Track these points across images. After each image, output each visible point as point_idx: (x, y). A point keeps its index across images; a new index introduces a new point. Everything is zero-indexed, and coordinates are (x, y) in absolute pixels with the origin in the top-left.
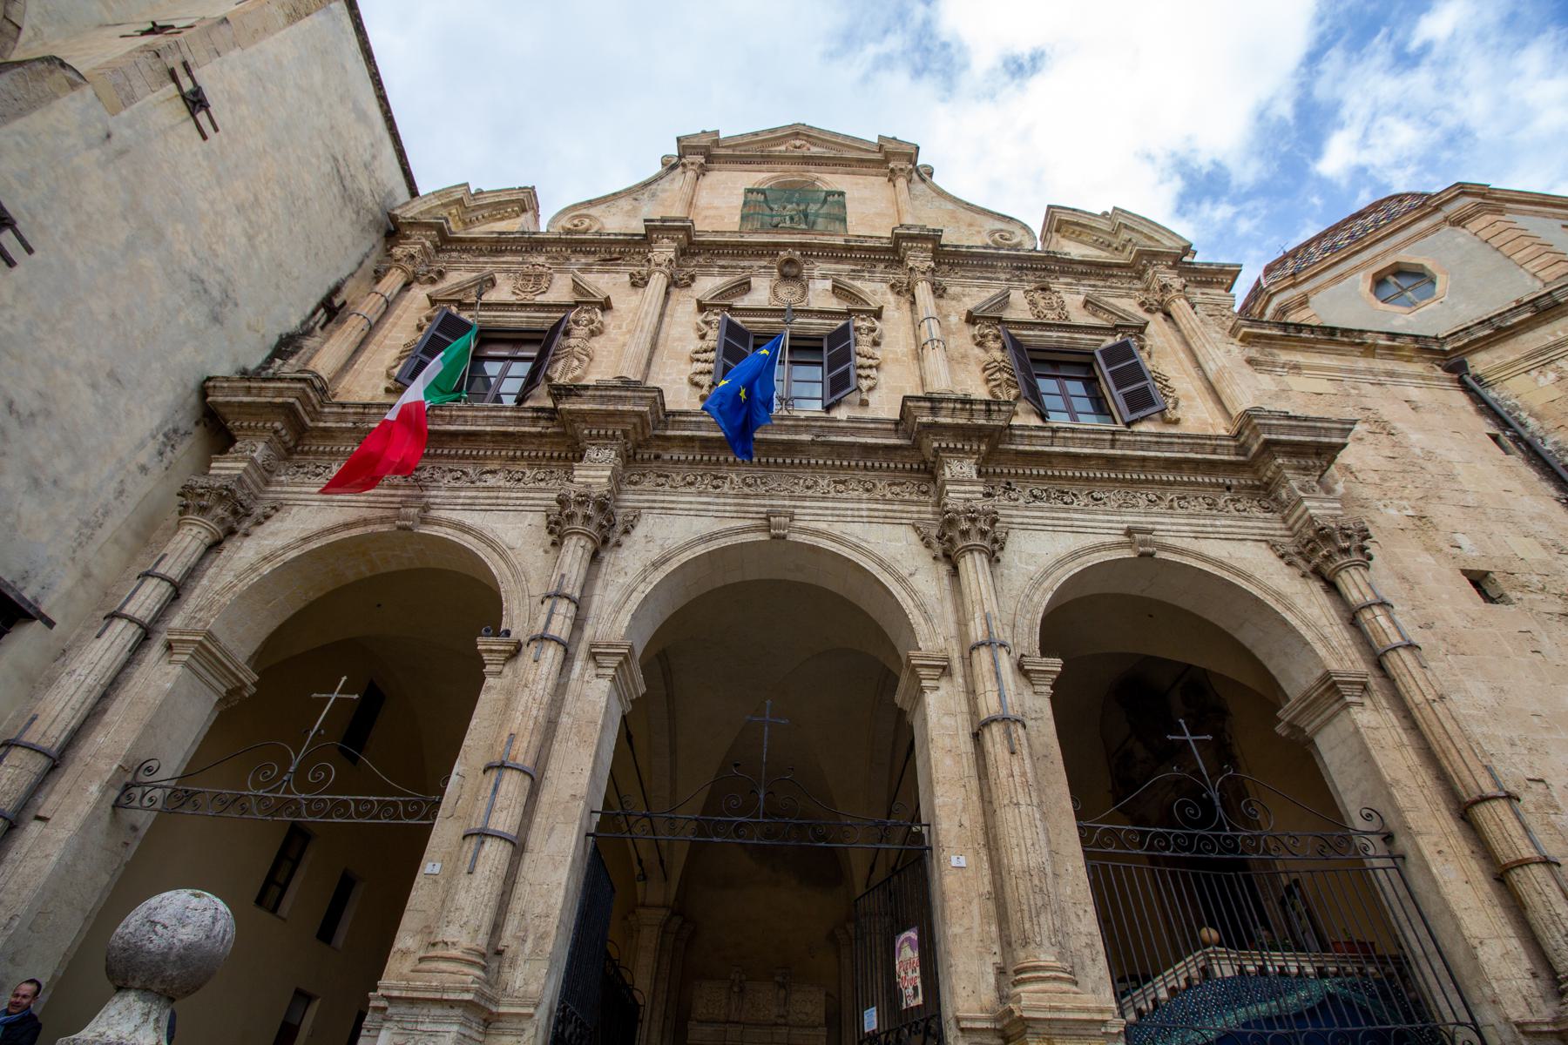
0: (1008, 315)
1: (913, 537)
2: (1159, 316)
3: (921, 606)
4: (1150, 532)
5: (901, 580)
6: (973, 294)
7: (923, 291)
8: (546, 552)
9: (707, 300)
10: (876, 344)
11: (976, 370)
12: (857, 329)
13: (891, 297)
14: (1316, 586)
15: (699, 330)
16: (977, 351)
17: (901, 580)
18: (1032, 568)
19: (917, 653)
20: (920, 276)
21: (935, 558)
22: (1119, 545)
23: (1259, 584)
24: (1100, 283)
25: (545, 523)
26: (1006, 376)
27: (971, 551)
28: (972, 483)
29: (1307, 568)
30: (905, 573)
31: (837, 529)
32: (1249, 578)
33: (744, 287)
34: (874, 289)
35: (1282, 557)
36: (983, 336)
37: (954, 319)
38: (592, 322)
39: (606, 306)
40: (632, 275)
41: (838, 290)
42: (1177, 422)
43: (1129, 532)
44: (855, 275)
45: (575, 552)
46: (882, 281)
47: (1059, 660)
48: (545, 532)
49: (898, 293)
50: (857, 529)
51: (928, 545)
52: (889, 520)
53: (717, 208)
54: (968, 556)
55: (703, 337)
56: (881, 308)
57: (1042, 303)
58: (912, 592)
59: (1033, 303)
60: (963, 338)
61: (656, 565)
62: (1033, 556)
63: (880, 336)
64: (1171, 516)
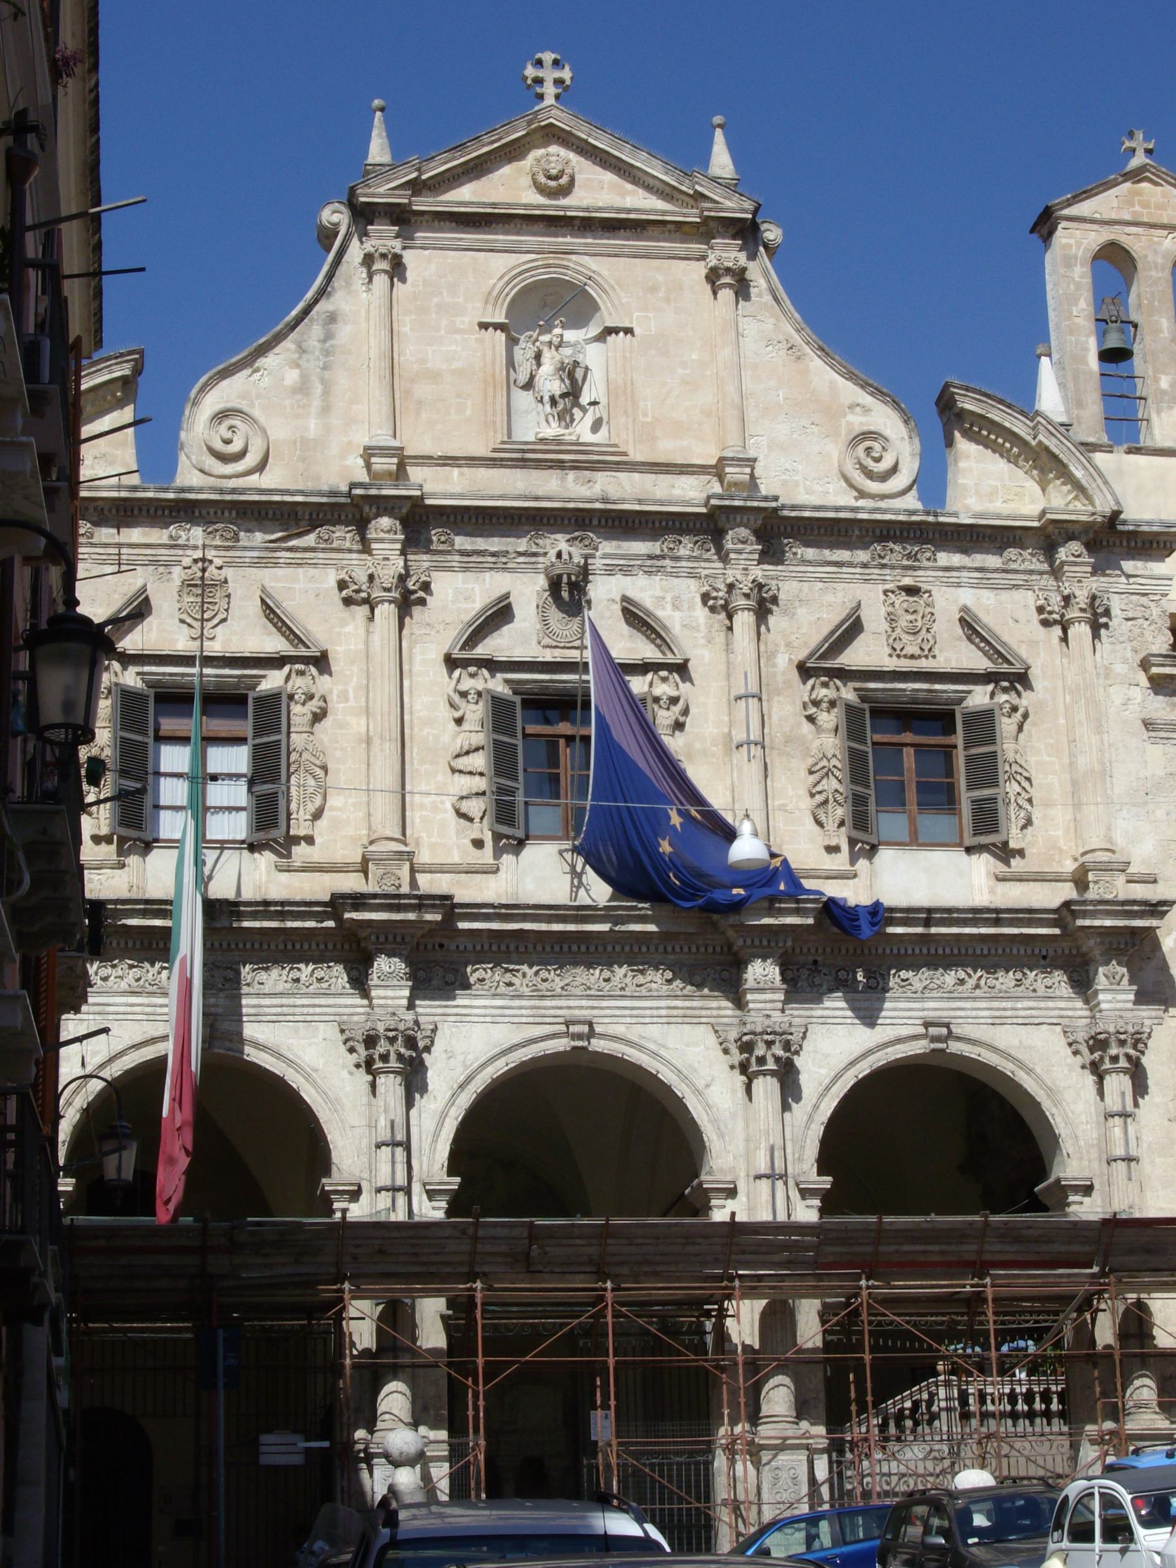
0: (856, 656)
1: (712, 1040)
2: (1057, 631)
3: (714, 1121)
4: (947, 1026)
5: (698, 1092)
6: (815, 596)
7: (744, 620)
8: (351, 1074)
9: (457, 654)
10: (679, 726)
11: (800, 766)
12: (657, 700)
13: (701, 614)
14: (1090, 1079)
15: (452, 705)
16: (807, 727)
17: (698, 1092)
18: (823, 1071)
19: (709, 1178)
20: (743, 602)
21: (732, 1067)
22: (915, 1037)
23: (1038, 1079)
24: (992, 561)
25: (340, 1038)
26: (835, 784)
27: (765, 1075)
28: (773, 990)
29: (1088, 1057)
30: (700, 1084)
31: (633, 1034)
32: (1030, 1071)
33: (500, 614)
34: (675, 594)
35: (1070, 1045)
36: (816, 703)
37: (783, 664)
38: (311, 697)
39: (321, 662)
40: (342, 585)
41: (636, 618)
42: (1021, 853)
43: (927, 1025)
44: (652, 565)
45: (391, 1087)
46: (693, 576)
47: (830, 1179)
48: (343, 1049)
49: (713, 609)
50: (654, 1031)
51: (726, 1051)
52: (689, 1019)
53: (434, 377)
54: (761, 1078)
55: (459, 721)
56: (687, 661)
57: (904, 621)
58: (708, 1106)
59: (891, 619)
60: (788, 701)
61: (462, 1086)
62: (827, 1056)
63: (686, 712)
64: (974, 999)
